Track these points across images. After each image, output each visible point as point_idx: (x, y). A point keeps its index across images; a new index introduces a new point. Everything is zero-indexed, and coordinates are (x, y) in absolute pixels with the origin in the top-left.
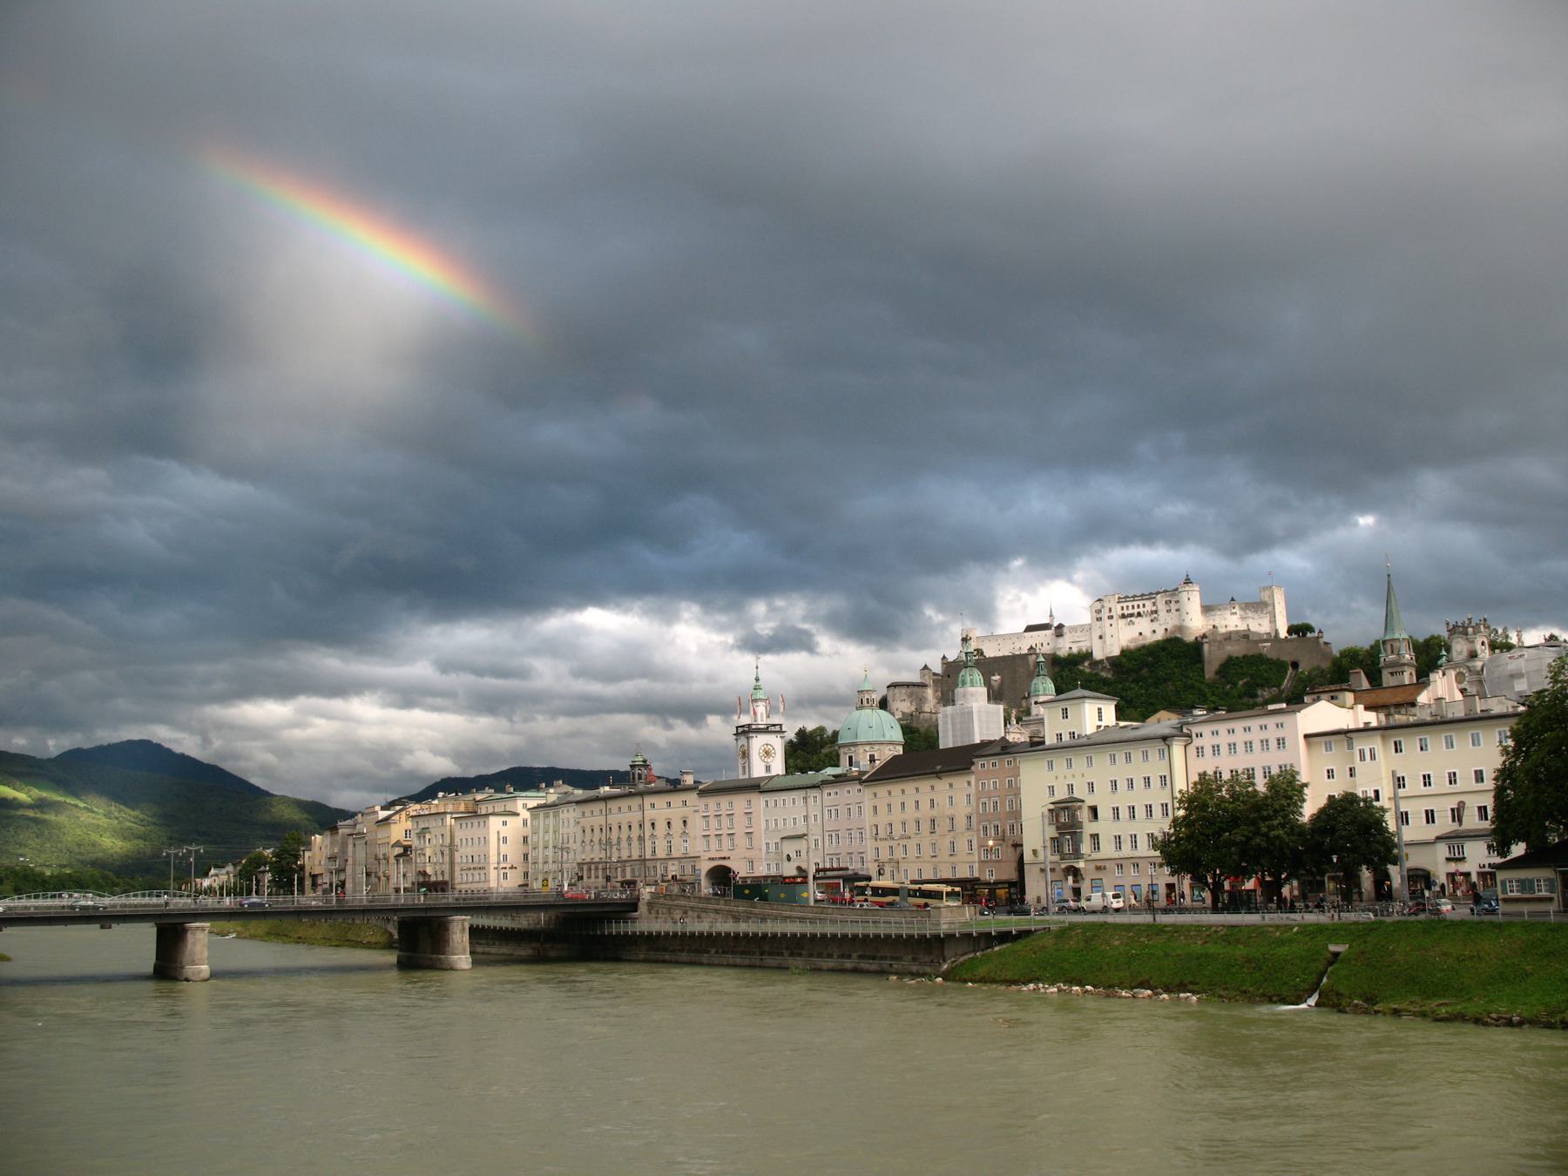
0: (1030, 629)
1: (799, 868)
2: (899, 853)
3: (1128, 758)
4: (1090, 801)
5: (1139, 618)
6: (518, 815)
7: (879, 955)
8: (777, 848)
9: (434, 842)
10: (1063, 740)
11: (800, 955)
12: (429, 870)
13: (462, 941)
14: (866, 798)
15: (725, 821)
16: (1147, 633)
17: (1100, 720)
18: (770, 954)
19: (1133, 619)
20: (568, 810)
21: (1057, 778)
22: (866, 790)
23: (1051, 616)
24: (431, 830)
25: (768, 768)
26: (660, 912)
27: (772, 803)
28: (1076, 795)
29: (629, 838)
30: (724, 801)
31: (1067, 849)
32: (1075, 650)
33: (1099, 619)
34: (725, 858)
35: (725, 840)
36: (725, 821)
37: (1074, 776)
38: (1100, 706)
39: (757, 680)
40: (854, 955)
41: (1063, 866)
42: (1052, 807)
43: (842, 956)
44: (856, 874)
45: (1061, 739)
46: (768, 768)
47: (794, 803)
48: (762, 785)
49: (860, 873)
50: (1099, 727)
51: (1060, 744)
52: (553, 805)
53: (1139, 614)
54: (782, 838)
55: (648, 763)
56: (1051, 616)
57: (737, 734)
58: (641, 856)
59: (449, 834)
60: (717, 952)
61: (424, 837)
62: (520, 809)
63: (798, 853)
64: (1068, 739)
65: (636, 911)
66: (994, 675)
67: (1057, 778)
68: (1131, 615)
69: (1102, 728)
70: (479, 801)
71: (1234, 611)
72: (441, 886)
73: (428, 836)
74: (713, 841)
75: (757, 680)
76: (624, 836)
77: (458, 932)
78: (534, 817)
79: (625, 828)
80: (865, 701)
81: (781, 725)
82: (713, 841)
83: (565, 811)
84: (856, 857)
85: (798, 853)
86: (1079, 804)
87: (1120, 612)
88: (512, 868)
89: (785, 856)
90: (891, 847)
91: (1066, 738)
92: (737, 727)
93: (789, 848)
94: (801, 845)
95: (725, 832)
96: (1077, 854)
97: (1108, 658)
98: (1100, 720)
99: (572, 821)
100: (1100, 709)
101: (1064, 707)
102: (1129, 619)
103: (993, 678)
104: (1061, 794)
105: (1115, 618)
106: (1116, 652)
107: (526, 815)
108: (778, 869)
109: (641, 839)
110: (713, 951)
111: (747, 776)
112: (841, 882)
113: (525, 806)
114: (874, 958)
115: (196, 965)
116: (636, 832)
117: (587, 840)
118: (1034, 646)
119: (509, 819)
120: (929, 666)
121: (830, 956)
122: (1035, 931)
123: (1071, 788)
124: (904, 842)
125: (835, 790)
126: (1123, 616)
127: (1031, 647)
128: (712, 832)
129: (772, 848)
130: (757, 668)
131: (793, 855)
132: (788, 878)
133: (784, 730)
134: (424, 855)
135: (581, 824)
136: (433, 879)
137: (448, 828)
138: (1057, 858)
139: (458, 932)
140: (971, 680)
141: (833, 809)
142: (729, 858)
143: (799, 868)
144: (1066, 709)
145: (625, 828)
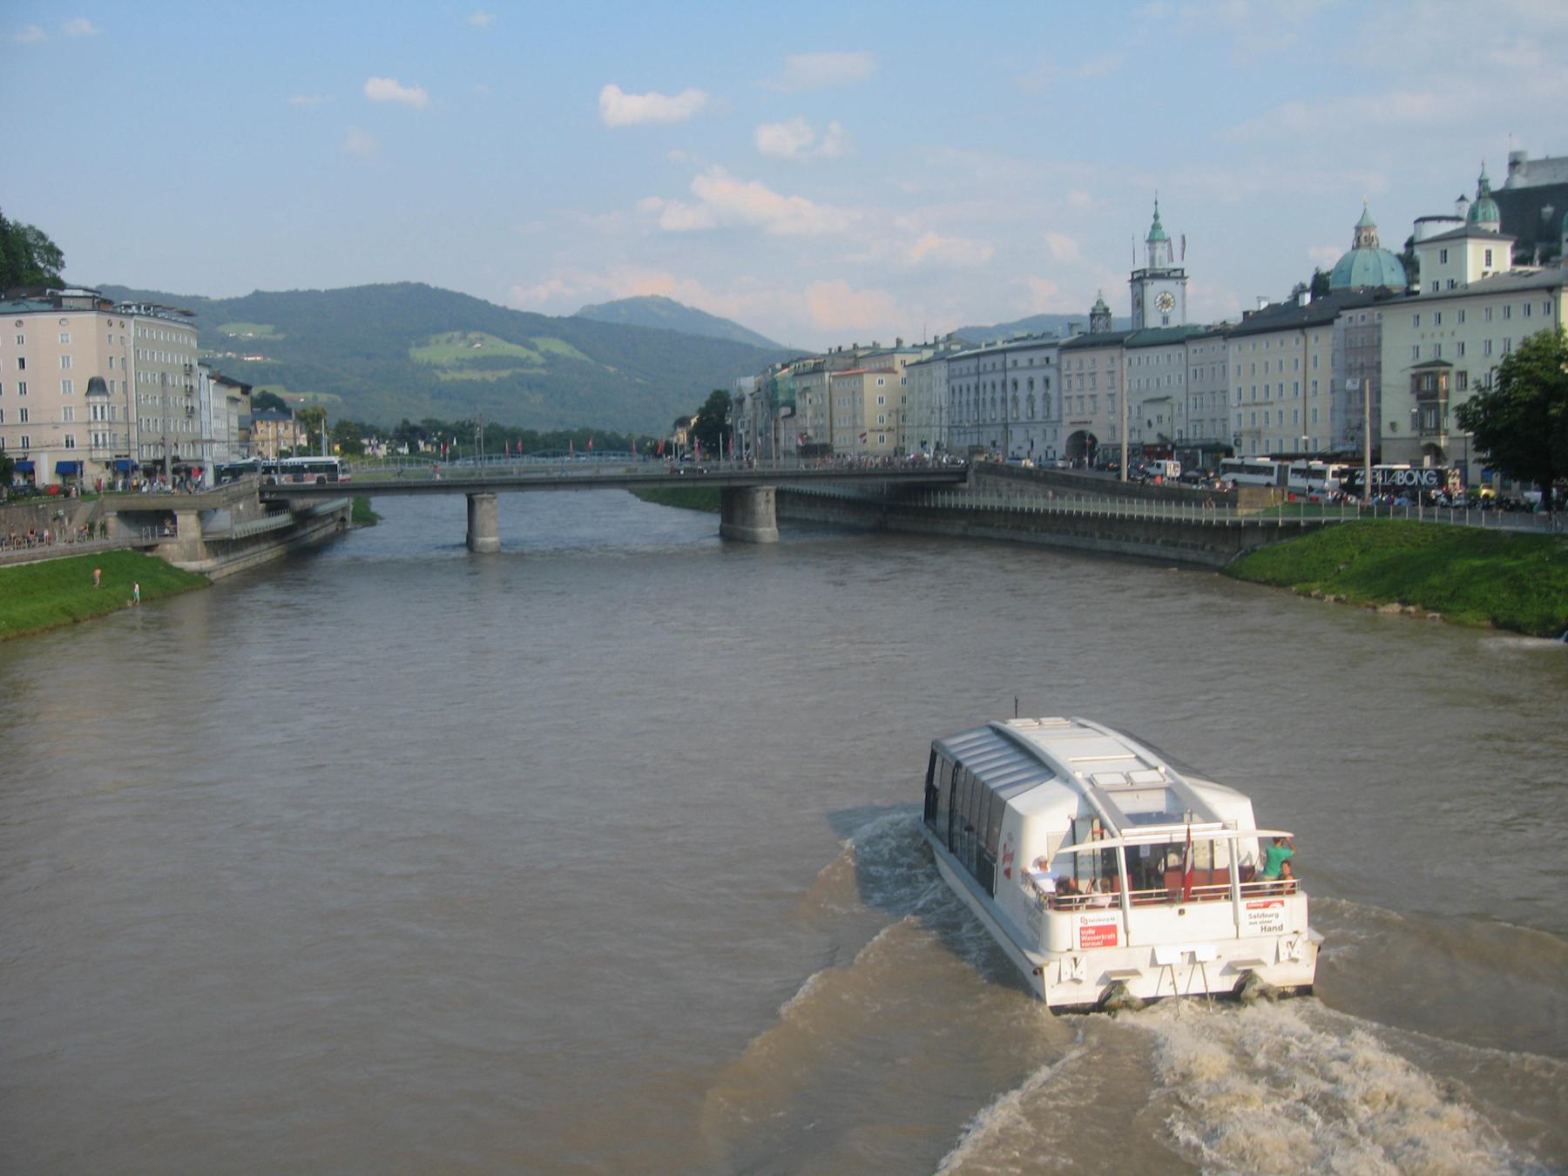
1: (1160, 435)
2: (1260, 422)
3: (1508, 312)
4: (1458, 366)
7: (1181, 541)
8: (1139, 412)
9: (814, 401)
10: (1440, 289)
11: (1110, 537)
12: (810, 432)
13: (767, 514)
14: (1231, 354)
15: (1088, 383)
17: (1489, 263)
18: (1085, 534)
20: (940, 368)
21: (1423, 336)
24: (812, 389)
25: (1166, 320)
26: (987, 483)
27: (1135, 362)
28: (1444, 358)
29: (993, 400)
30: (1087, 357)
31: (1429, 422)
34: (1086, 422)
35: (1087, 400)
36: (1088, 383)
37: (1442, 334)
38: (1489, 247)
39: (1156, 217)
40: (1159, 542)
41: (1423, 443)
42: (1413, 371)
43: (1147, 541)
44: (1218, 444)
45: (1438, 288)
46: (1166, 320)
47: (1158, 361)
48: (1125, 340)
49: (1223, 443)
50: (1485, 274)
51: (1436, 294)
52: (928, 362)
54: (1145, 402)
55: (1110, 311)
57: (1132, 281)
58: (1003, 419)
59: (827, 393)
60: (1036, 531)
61: (805, 396)
62: (898, 367)
63: (1160, 418)
64: (1446, 287)
65: (965, 481)
66: (1545, 206)
67: (1423, 336)
69: (1490, 275)
70: (861, 357)
72: (825, 450)
73: (808, 396)
74: (1075, 402)
75: (1156, 217)
76: (988, 397)
77: (763, 503)
78: (910, 375)
79: (989, 388)
80: (1362, 238)
81: (1183, 271)
82: (1075, 402)
83: (937, 367)
84: (1219, 427)
85: (1160, 418)
86: (1443, 369)
88: (889, 430)
89: (1146, 421)
90: (1253, 414)
91: (1443, 287)
92: (1133, 274)
93: (1150, 413)
94: (1164, 410)
95: (1087, 393)
96: (1437, 430)
98: (1489, 263)
99: (943, 382)
100: (1489, 253)
101: (1444, 249)
104: (1426, 356)
107: (902, 373)
108: (1139, 436)
109: (1004, 400)
110: (1033, 529)
111: (1141, 327)
112: (1200, 452)
113: (903, 362)
114: (1175, 545)
115: (487, 537)
116: (999, 394)
117: (957, 400)
119: (884, 377)
120: (1466, 196)
121: (1137, 540)
122: (1326, 523)
123: (1439, 348)
124: (1268, 408)
125: (1202, 346)
128: (1074, 393)
129: (1134, 409)
130: (1156, 203)
131: (1154, 421)
132: (1149, 446)
133: (1185, 274)
134: (806, 416)
135: (951, 385)
136: (816, 441)
137: (827, 387)
138: (1415, 434)
139: (763, 503)
140: (1484, 214)
141: (1198, 368)
142: (1091, 422)
143: (1160, 435)
144: (1446, 252)
145: (989, 388)
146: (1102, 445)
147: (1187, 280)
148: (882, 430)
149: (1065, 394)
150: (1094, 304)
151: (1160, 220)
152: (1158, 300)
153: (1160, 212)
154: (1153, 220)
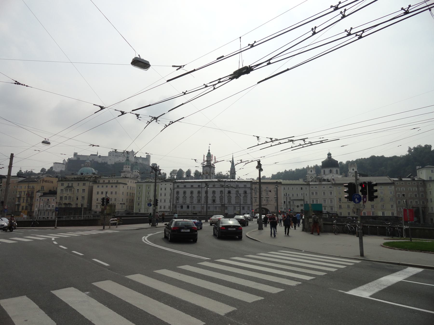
0: (91, 155)
5: (120, 157)
6: (126, 184)
16: (121, 160)
19: (118, 157)
22: (335, 187)
23: (97, 153)
32: (103, 162)
33: (110, 156)
39: (209, 150)
53: (120, 156)
56: (97, 153)
68: (118, 156)
71: (141, 159)
73: (73, 189)
75: (209, 150)
87: (116, 155)
97: (111, 164)
102: (117, 157)
103: (82, 165)
105: (114, 156)
106: (113, 163)
118: (94, 159)
119: (125, 186)
126: (116, 156)
127: (93, 159)
130: (209, 147)
146: (271, 212)
147: (215, 168)
148: (122, 204)
149: (253, 196)
150: (18, 171)
151: (210, 152)
152: (205, 172)
153: (210, 150)
154: (208, 152)
